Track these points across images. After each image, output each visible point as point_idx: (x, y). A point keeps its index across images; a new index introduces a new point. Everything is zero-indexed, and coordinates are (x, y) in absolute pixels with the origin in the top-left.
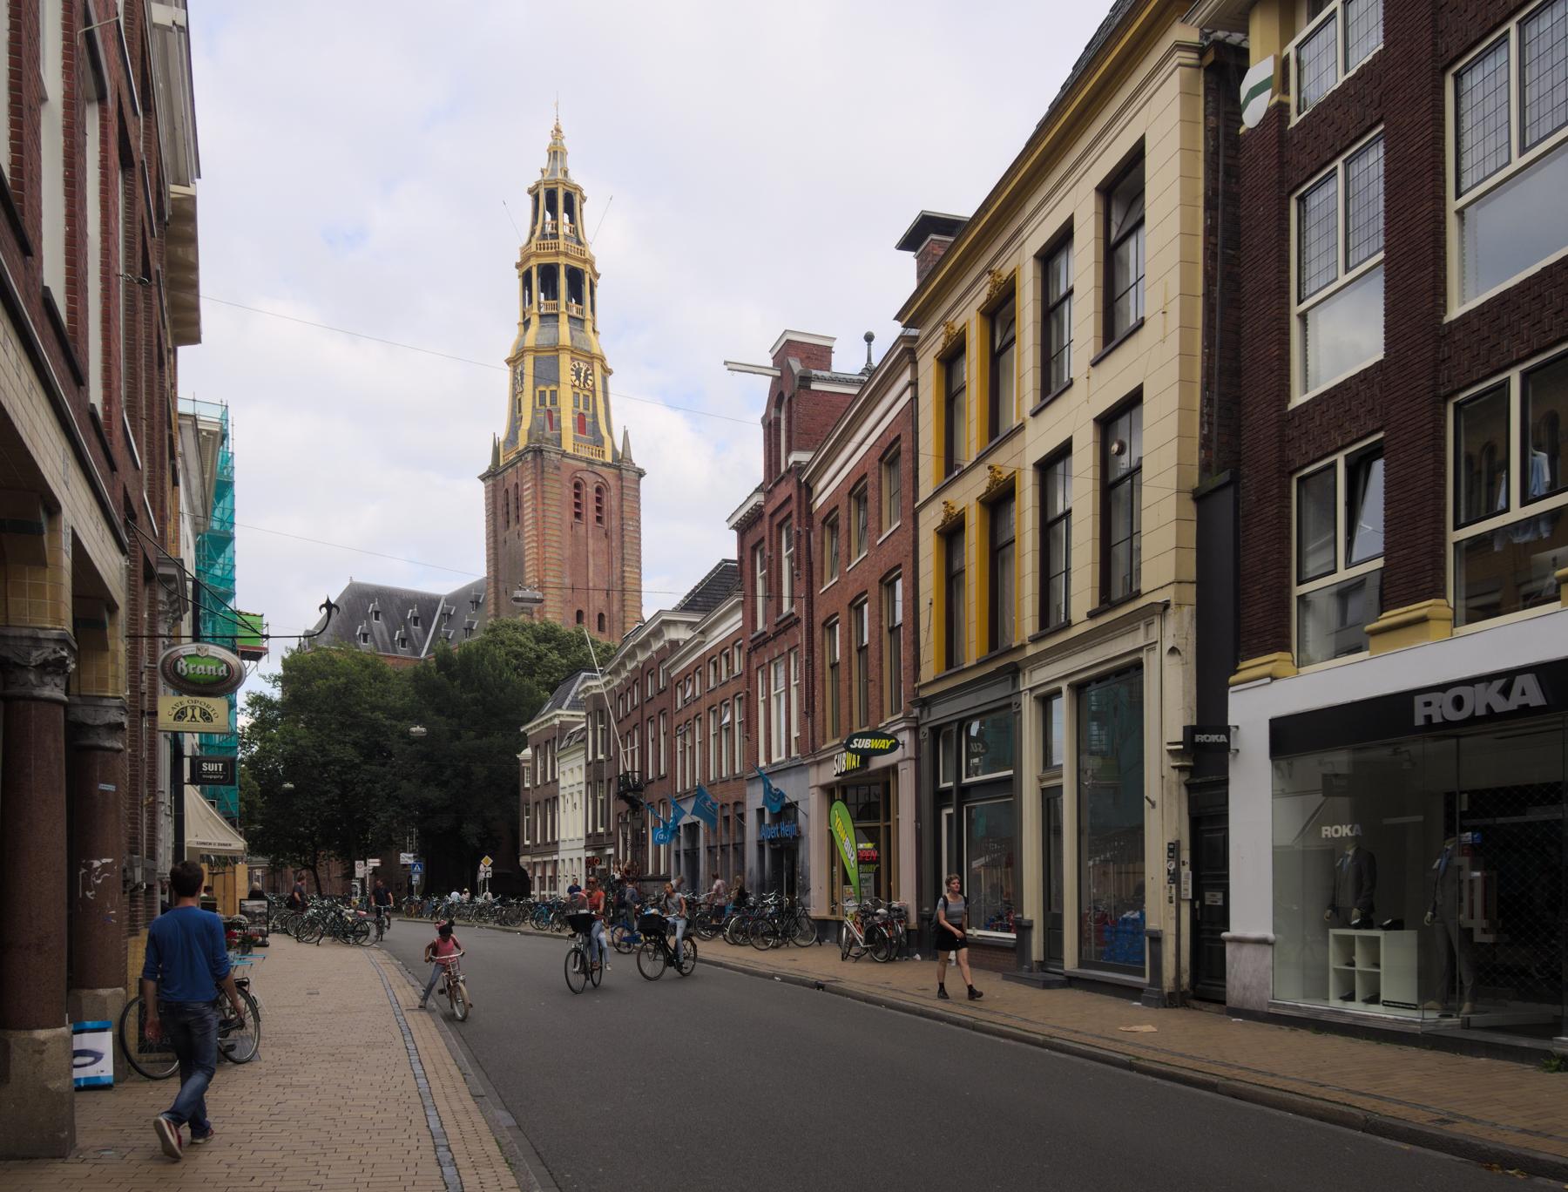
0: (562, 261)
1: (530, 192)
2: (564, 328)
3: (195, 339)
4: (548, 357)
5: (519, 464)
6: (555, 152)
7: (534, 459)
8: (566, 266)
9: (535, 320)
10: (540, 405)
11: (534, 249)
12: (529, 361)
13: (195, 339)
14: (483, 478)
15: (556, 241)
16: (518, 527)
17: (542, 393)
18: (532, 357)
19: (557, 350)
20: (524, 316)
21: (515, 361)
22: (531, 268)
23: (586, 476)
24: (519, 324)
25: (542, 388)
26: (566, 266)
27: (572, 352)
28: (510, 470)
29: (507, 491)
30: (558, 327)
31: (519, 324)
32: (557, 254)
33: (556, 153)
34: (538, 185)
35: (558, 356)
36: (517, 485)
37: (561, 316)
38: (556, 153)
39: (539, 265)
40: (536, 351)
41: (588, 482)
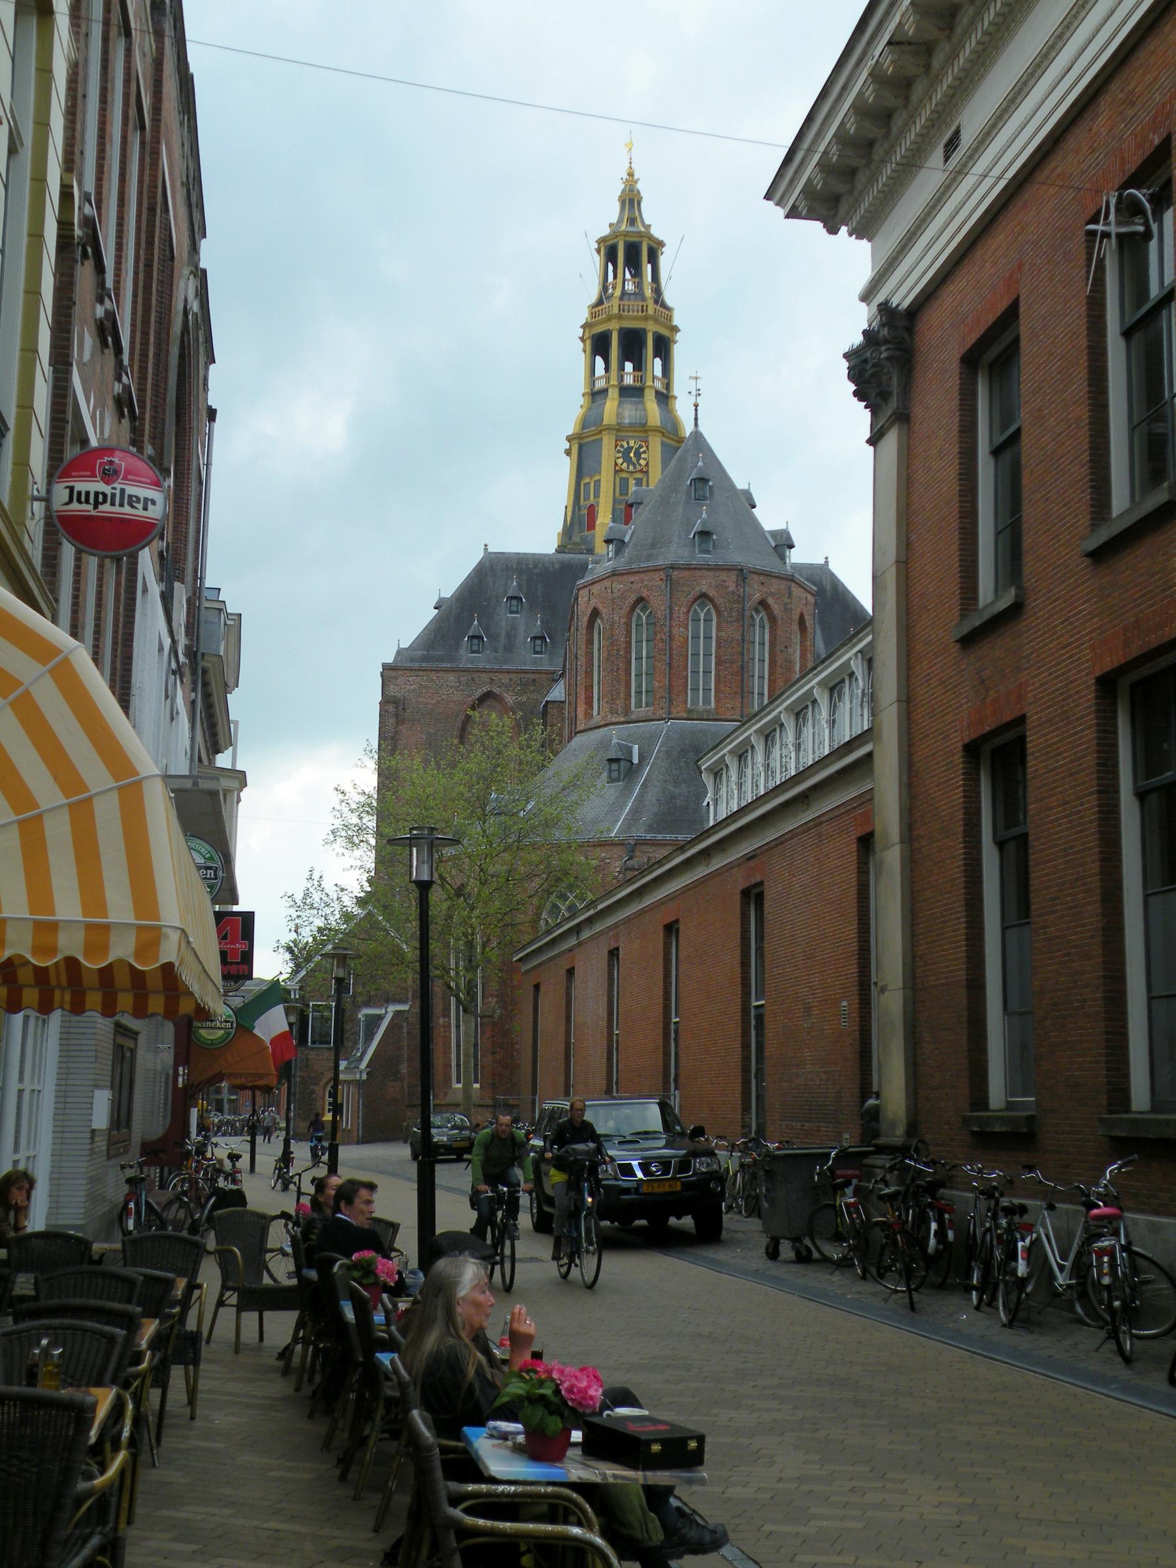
0: (651, 328)
1: (601, 241)
2: (652, 405)
3: (214, 362)
6: (631, 201)
8: (655, 333)
9: (613, 394)
10: (621, 494)
11: (615, 310)
12: (608, 443)
13: (214, 362)
19: (646, 431)
21: (581, 438)
24: (584, 395)
26: (655, 333)
27: (663, 434)
30: (643, 403)
31: (584, 395)
32: (646, 318)
33: (631, 200)
34: (615, 234)
38: (631, 200)
40: (618, 430)
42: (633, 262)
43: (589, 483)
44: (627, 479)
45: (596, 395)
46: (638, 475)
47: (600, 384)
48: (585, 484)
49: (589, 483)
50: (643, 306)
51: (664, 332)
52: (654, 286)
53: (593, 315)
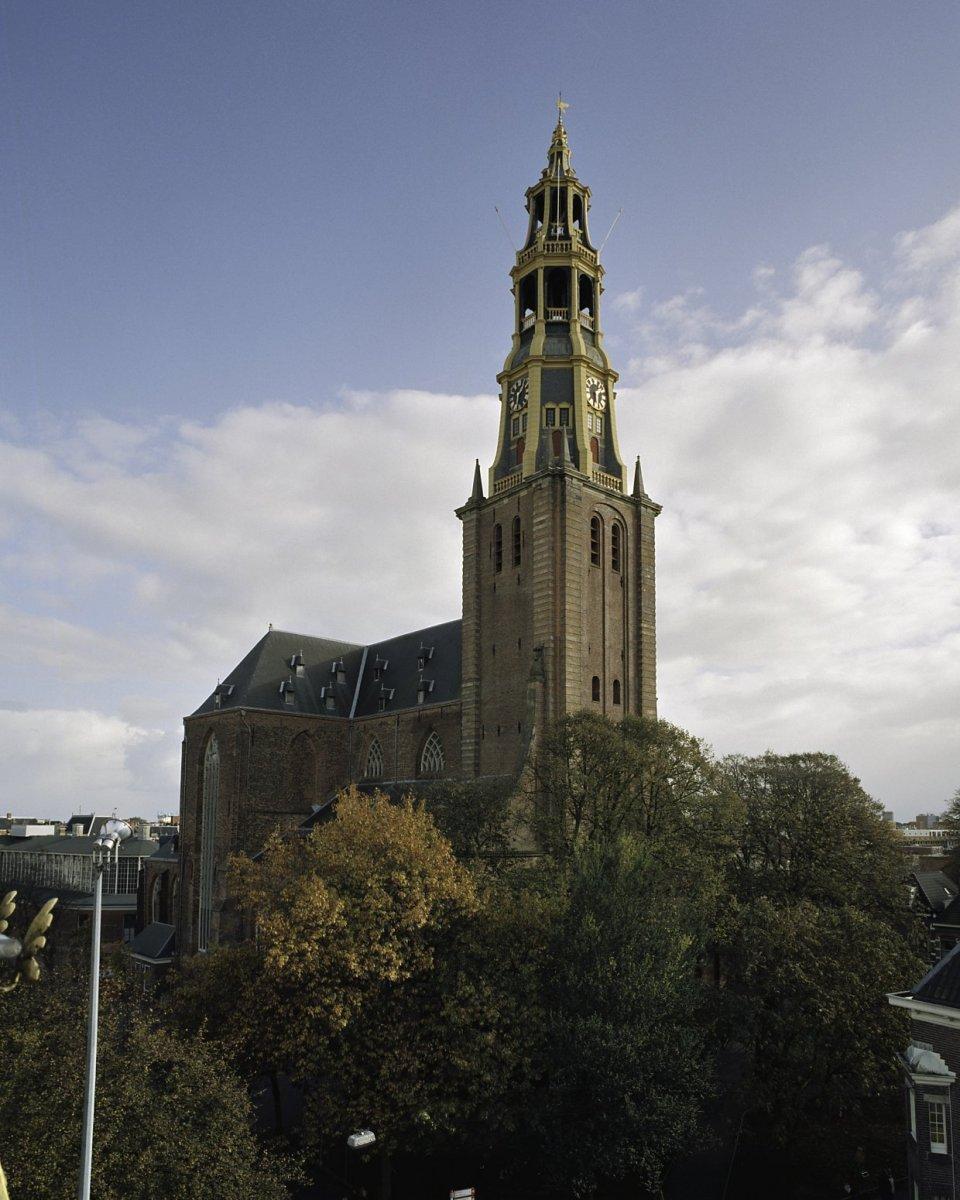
4: (558, 370)
5: (523, 493)
7: (553, 485)
14: (460, 513)
15: (568, 243)
16: (519, 570)
17: (551, 411)
18: (539, 369)
20: (521, 325)
21: (510, 376)
22: (536, 271)
23: (607, 513)
25: (550, 405)
28: (506, 501)
29: (499, 528)
33: (556, 155)
35: (572, 369)
36: (517, 521)
37: (572, 325)
39: (546, 269)
41: (606, 518)
42: (558, 212)
43: (518, 419)
44: (553, 409)
45: (525, 336)
46: (564, 405)
47: (527, 325)
48: (514, 420)
49: (518, 419)
50: (566, 245)
51: (591, 274)
52: (581, 232)
53: (521, 260)
